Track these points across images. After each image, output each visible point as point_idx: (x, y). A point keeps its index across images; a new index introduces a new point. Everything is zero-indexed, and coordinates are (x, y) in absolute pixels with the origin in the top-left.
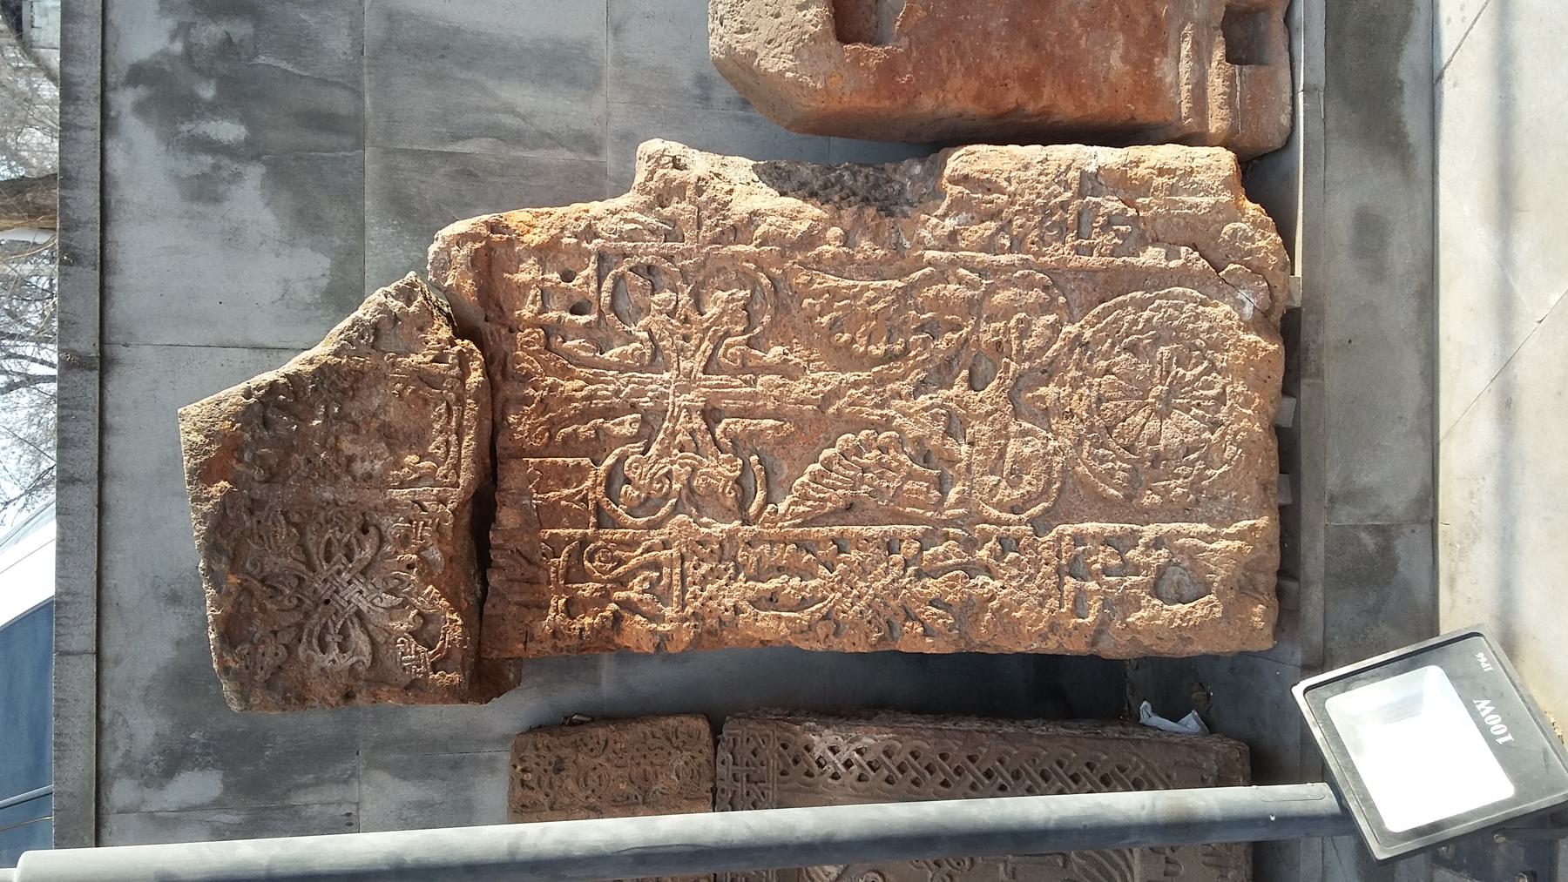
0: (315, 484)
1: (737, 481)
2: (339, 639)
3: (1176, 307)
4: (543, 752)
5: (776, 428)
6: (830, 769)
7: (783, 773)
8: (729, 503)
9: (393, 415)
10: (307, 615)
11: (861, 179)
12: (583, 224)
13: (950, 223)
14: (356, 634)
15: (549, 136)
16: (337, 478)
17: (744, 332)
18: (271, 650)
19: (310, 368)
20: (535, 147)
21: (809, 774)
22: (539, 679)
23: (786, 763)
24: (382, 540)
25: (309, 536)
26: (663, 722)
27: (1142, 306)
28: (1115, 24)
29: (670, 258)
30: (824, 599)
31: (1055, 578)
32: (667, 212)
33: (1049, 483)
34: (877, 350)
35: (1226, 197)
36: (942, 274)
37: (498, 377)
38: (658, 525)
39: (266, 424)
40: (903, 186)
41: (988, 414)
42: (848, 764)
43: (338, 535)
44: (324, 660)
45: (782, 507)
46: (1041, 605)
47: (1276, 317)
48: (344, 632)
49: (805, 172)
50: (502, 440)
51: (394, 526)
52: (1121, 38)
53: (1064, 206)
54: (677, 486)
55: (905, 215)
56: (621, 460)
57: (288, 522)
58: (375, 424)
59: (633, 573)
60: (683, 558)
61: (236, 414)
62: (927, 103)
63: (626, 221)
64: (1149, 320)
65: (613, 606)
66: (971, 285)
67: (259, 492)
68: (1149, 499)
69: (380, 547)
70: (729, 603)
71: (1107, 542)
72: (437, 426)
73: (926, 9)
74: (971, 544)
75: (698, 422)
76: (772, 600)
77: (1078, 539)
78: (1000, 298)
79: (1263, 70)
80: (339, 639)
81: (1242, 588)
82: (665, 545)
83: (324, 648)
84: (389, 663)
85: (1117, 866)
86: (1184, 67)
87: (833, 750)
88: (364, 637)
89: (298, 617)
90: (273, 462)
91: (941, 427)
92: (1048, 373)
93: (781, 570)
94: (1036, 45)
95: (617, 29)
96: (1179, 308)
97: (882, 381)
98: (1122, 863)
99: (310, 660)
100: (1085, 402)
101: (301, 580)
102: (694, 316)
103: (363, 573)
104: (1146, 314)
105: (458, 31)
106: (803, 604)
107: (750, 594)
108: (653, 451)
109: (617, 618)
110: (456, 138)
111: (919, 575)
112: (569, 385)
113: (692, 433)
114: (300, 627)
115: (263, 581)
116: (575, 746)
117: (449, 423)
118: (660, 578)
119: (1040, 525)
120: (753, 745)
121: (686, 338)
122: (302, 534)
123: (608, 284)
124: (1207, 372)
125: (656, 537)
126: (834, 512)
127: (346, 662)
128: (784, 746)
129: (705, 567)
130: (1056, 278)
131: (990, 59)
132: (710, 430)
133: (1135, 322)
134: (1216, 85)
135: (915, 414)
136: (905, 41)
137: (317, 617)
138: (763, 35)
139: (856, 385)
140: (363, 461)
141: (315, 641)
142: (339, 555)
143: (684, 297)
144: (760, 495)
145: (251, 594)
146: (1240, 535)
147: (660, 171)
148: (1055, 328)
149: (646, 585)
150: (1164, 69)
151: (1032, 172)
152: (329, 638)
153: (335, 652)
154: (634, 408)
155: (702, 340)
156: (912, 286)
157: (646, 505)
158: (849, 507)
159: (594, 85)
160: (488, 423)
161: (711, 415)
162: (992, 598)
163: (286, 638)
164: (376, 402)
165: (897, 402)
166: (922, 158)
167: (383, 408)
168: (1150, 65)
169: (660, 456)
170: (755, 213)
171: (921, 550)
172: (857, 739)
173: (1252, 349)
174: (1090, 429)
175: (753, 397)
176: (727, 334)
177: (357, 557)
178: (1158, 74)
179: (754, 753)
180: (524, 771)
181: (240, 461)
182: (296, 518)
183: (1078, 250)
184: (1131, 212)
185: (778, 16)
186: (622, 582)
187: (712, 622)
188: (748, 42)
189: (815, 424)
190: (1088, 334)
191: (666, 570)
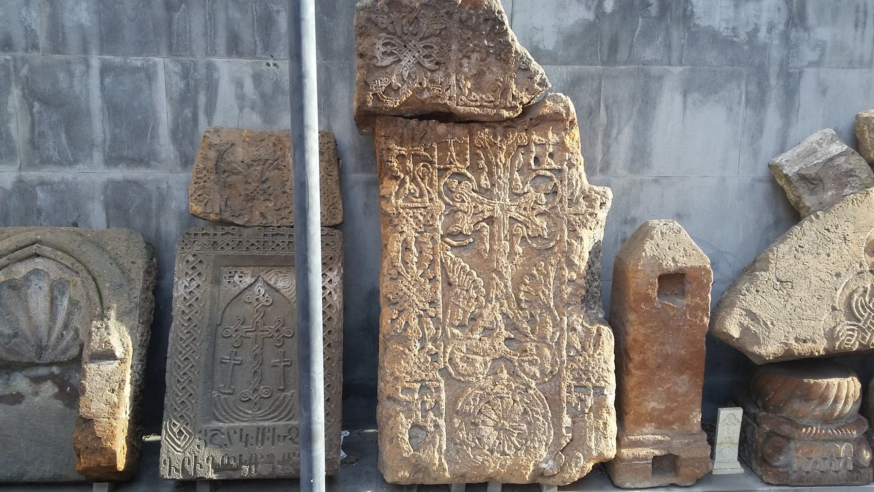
0: (459, 42)
1: (461, 232)
3: (544, 432)
4: (326, 146)
5: (485, 250)
8: (451, 229)
9: (489, 77)
10: (399, 37)
11: (596, 290)
12: (575, 162)
13: (579, 328)
15: (608, 150)
16: (461, 51)
17: (528, 235)
18: (385, 21)
19: (510, 40)
20: (603, 143)
22: (358, 145)
24: (432, 71)
25: (435, 39)
26: (340, 202)
27: (545, 416)
28: (669, 404)
29: (561, 202)
30: (408, 273)
31: (419, 379)
32: (581, 200)
33: (463, 375)
34: (522, 296)
35: (594, 454)
36: (557, 325)
37: (505, 124)
38: (440, 197)
39: (486, 20)
40: (593, 309)
41: (494, 347)
44: (379, 45)
45: (449, 253)
46: (407, 373)
47: (540, 480)
48: (392, 53)
49: (598, 265)
50: (477, 125)
51: (439, 76)
52: (663, 407)
53: (589, 379)
54: (458, 205)
55: (582, 308)
56: (469, 179)
58: (485, 69)
59: (418, 185)
60: (425, 208)
61: (491, 7)
62: (632, 317)
63: (577, 181)
64: (538, 420)
65: (402, 176)
66: (552, 338)
67: (456, 17)
68: (457, 421)
69: (429, 70)
70: (405, 229)
71: (436, 402)
72: (484, 96)
73: (674, 316)
74: (434, 340)
75: (487, 214)
76: (407, 249)
77: (438, 389)
78: (547, 352)
79: (650, 474)
80: (389, 51)
81: (417, 466)
82: (431, 200)
83: (385, 45)
84: (377, 74)
85: (280, 414)
86: (651, 437)
87: (330, 281)
88: (389, 63)
89: (399, 33)
90: (469, 23)
91: (487, 326)
92: (513, 374)
93: (421, 253)
94: (659, 367)
95: (656, 181)
96: (544, 433)
97: (507, 298)
98: (282, 416)
99: (379, 38)
100: (500, 391)
101: (416, 35)
102: (535, 213)
103: (418, 63)
104: (541, 418)
105: (654, 108)
106: (405, 263)
107: (409, 239)
108: (474, 194)
109: (397, 178)
110: (607, 107)
111: (420, 316)
112: (502, 156)
113: (483, 212)
114: (394, 34)
115: (416, 18)
116: (329, 161)
118: (416, 197)
119: (444, 372)
121: (525, 209)
122: (436, 36)
123: (548, 173)
124: (516, 447)
125: (435, 196)
126: (448, 277)
127: (378, 54)
128: (331, 258)
129: (421, 218)
130: (556, 377)
131: (653, 346)
132: (484, 220)
133: (537, 413)
134: (643, 452)
135: (493, 313)
136: (660, 306)
137: (398, 41)
138: (661, 243)
139: (506, 286)
143: (543, 208)
144: (455, 243)
145: (410, 12)
146: (441, 464)
147: (599, 197)
148: (534, 377)
149: (412, 191)
150: (649, 428)
151: (603, 365)
153: (383, 49)
154: (493, 185)
155: (524, 216)
156: (551, 311)
157: (449, 190)
158: (450, 284)
159: (631, 170)
160: (485, 119)
161: (491, 220)
162: (410, 350)
163: (390, 28)
164: (494, 69)
165: (498, 305)
166: (605, 318)
167: (492, 72)
168: (651, 421)
169: (471, 197)
170: (582, 239)
171: (431, 317)
172: (336, 292)
173: (526, 468)
174: (488, 394)
175: (500, 240)
176: (527, 227)
178: (647, 425)
181: (470, 8)
182: (443, 33)
183: (569, 386)
184: (587, 411)
186: (414, 180)
187: (396, 221)
188: (657, 236)
189: (487, 267)
190: (532, 392)
191: (420, 200)
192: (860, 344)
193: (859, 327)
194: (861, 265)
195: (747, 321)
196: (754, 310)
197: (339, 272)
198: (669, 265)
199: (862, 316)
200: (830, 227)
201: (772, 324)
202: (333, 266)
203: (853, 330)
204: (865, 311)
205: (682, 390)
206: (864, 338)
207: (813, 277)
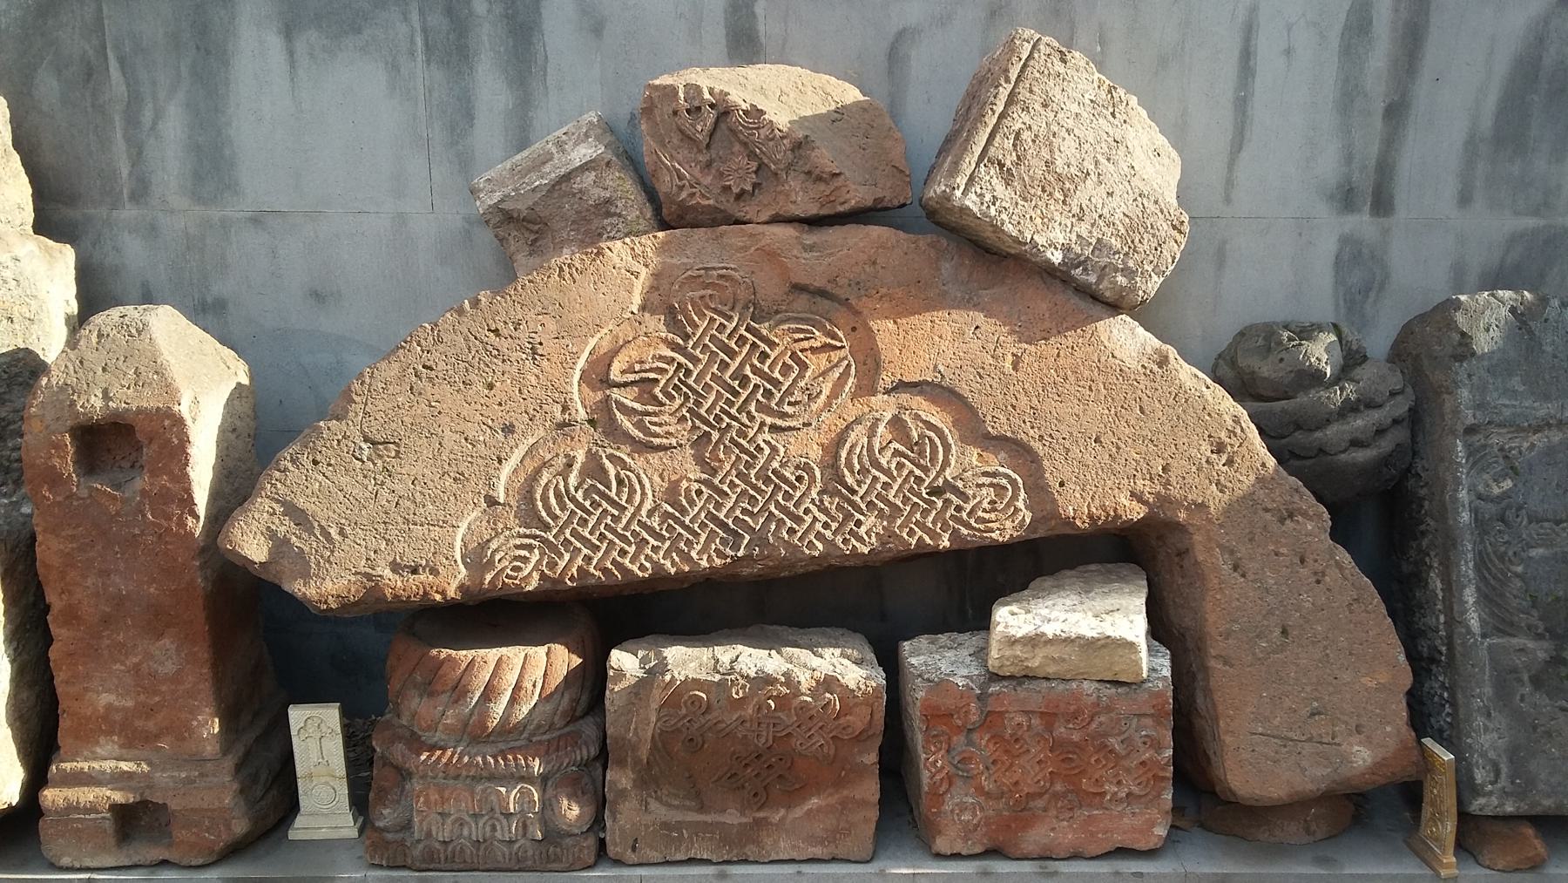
15: (140, 153)
20: (128, 140)
28: (142, 697)
52: (130, 704)
73: (118, 514)
79: (112, 841)
86: (108, 765)
94: (106, 620)
95: (257, 220)
105: (226, 64)
110: (122, 61)
131: (85, 577)
134: (86, 795)
136: (84, 493)
150: (107, 746)
159: (198, 199)
168: (110, 733)
178: (102, 740)
185: (104, 370)
192: (543, 576)
193: (544, 541)
194: (565, 409)
195: (284, 527)
196: (301, 502)
198: (93, 404)
199: (555, 518)
200: (500, 326)
201: (342, 533)
203: (530, 548)
204: (563, 508)
205: (169, 668)
206: (552, 565)
207: (447, 432)
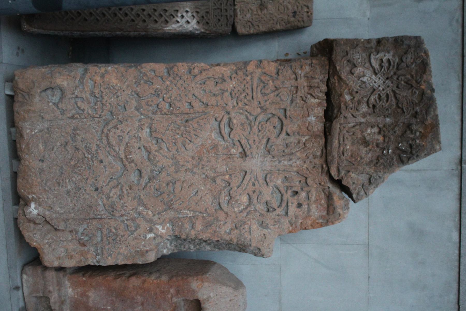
0: (392, 124)
2: (383, 64)
4: (301, 19)
6: (190, 14)
7: (207, 12)
9: (364, 150)
10: (395, 73)
11: (187, 247)
14: (376, 66)
16: (384, 126)
18: (409, 60)
21: (197, 12)
23: (206, 16)
25: (394, 104)
26: (255, 32)
37: (324, 166)
40: (170, 245)
42: (183, 17)
43: (384, 104)
44: (389, 56)
47: (22, 202)
48: (381, 66)
49: (208, 248)
50: (322, 142)
51: (364, 108)
55: (170, 236)
57: (402, 109)
58: (370, 147)
62: (164, 278)
67: (413, 121)
69: (368, 100)
80: (383, 64)
83: (389, 61)
84: (364, 55)
87: (188, 22)
88: (373, 65)
89: (399, 73)
90: (408, 132)
99: (393, 56)
103: (374, 90)
114: (398, 69)
115: (412, 86)
116: (289, 22)
117: (343, 148)
120: (220, 23)
122: (397, 104)
127: (380, 55)
128: (207, 23)
131: (141, 295)
137: (392, 72)
140: (374, 133)
141: (392, 63)
142: (384, 96)
145: (416, 81)
152: (387, 64)
160: (329, 148)
164: (370, 155)
167: (367, 153)
177: (377, 96)
179: (219, 20)
180: (308, 12)
181: (420, 132)
182: (399, 110)
187: (240, 73)
197: (197, 30)
202: (201, 25)
